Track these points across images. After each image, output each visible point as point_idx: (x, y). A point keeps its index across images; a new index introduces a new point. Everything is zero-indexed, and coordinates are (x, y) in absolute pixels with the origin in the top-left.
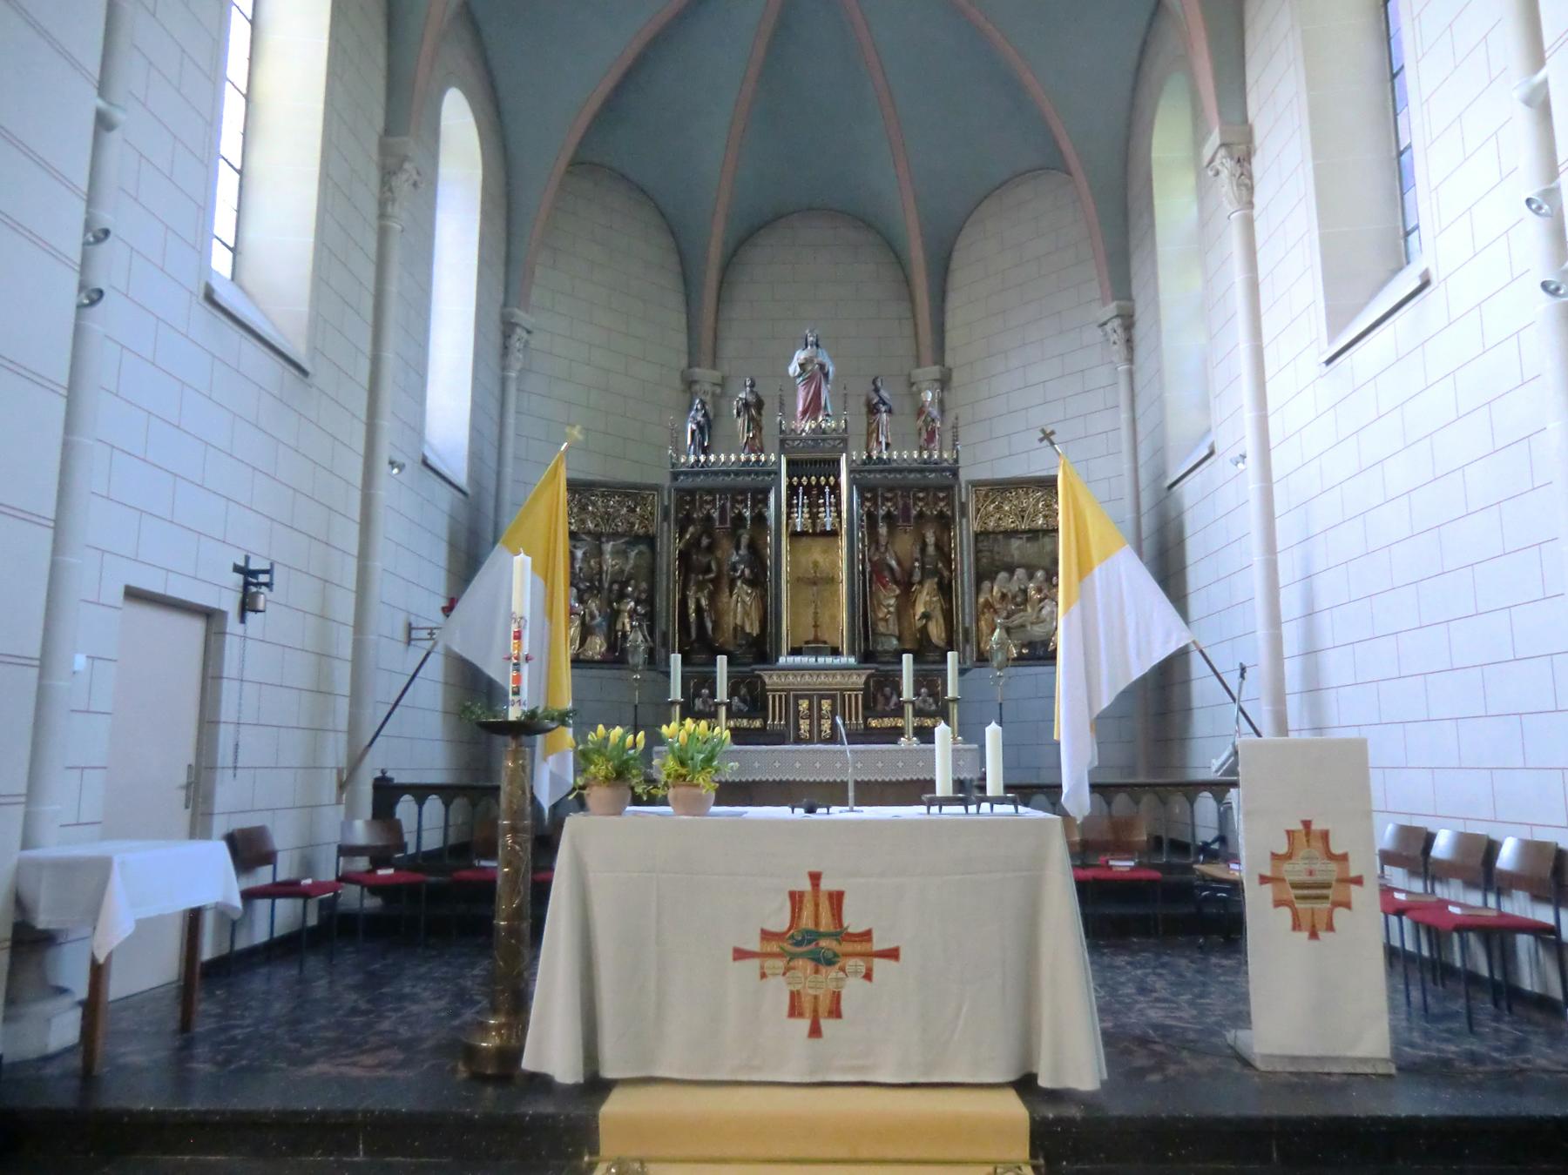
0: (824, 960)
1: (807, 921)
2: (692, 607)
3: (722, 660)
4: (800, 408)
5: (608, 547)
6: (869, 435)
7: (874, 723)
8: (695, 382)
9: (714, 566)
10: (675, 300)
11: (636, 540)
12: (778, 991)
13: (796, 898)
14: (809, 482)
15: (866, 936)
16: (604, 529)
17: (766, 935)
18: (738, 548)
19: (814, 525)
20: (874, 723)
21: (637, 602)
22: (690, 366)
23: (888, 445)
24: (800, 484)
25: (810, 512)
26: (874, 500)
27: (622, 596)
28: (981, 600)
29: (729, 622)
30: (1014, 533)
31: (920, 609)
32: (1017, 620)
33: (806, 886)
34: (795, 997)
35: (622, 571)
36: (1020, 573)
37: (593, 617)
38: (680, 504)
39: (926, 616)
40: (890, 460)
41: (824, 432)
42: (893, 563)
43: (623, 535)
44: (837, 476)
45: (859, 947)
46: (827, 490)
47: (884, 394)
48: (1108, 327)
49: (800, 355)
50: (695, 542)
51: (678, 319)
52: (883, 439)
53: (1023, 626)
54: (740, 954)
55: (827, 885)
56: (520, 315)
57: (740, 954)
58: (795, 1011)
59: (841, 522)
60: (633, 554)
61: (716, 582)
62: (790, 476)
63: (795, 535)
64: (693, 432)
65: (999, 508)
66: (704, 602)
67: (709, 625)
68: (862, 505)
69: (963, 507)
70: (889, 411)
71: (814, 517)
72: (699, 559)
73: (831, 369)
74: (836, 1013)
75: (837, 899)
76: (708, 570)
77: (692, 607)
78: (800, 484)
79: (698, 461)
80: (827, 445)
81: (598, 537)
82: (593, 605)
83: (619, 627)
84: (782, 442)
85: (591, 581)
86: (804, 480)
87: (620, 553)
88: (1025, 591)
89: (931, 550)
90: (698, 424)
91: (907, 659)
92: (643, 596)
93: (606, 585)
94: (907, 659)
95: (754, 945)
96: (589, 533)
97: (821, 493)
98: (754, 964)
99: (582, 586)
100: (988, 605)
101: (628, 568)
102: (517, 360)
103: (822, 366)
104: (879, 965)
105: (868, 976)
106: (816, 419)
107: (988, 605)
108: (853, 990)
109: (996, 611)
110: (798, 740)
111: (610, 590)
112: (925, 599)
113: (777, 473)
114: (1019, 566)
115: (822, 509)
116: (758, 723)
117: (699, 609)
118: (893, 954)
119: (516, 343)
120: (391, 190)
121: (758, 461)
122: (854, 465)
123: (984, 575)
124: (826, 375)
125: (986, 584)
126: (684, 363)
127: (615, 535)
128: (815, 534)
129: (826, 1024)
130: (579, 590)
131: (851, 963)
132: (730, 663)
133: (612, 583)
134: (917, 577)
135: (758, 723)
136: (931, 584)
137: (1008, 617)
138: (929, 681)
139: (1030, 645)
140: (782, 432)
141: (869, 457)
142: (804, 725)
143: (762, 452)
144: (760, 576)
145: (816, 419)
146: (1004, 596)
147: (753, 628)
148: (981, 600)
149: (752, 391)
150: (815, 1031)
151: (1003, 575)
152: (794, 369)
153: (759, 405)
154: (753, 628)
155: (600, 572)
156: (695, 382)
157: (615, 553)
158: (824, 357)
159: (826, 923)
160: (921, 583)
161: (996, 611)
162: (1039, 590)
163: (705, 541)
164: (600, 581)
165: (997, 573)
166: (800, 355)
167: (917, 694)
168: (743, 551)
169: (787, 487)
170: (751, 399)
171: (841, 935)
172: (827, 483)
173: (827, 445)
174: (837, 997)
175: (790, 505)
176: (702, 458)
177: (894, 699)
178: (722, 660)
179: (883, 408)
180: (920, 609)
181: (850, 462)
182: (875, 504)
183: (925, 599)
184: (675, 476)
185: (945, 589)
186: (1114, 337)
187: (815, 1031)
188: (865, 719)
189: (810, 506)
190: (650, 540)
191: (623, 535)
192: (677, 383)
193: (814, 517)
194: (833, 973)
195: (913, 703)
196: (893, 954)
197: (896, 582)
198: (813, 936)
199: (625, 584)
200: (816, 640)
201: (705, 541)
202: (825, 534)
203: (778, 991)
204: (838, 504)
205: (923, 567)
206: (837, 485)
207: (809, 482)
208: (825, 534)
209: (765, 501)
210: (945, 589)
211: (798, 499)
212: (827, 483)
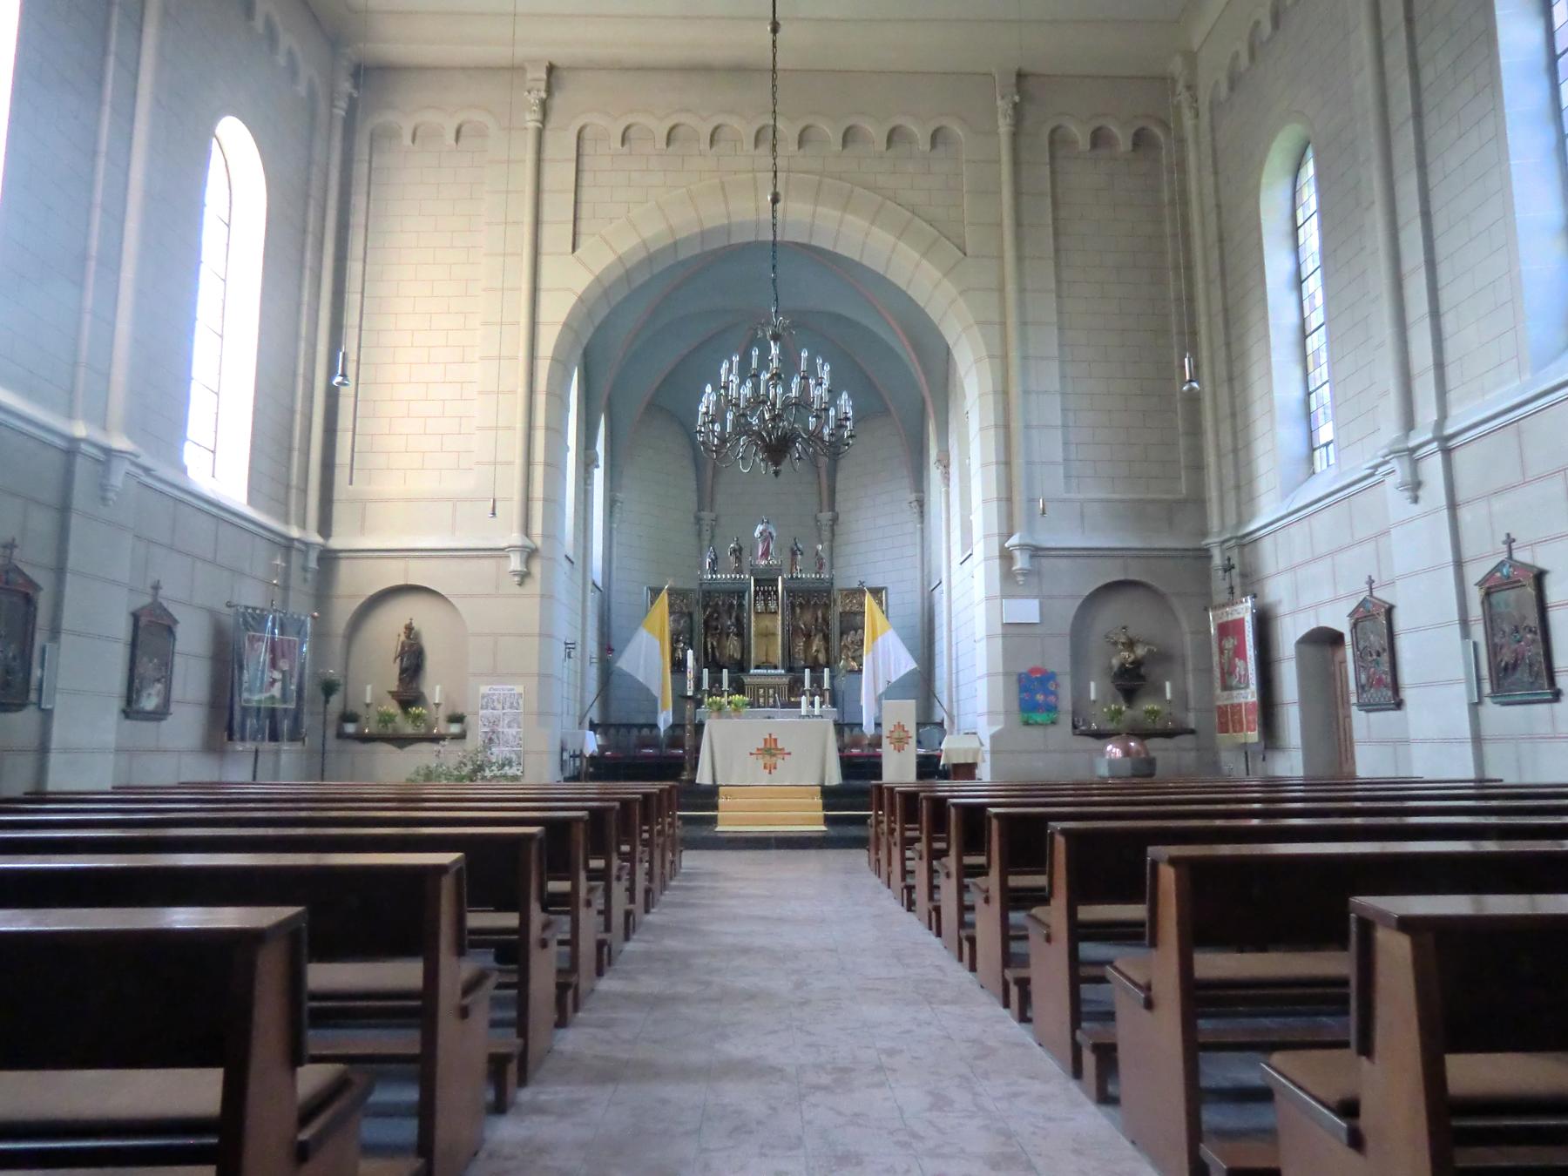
0: (774, 755)
1: (768, 746)
2: (709, 646)
3: (725, 671)
4: (760, 553)
6: (792, 565)
7: (793, 699)
8: (702, 519)
9: (719, 627)
12: (761, 763)
13: (765, 740)
17: (758, 749)
18: (730, 618)
19: (766, 609)
20: (793, 699)
22: (699, 510)
23: (800, 570)
24: (760, 590)
26: (794, 597)
28: (842, 644)
31: (814, 648)
33: (768, 737)
34: (765, 764)
35: (677, 630)
38: (704, 596)
39: (817, 651)
40: (801, 578)
41: (771, 566)
42: (803, 626)
47: (800, 546)
48: (912, 505)
49: (760, 528)
50: (711, 615)
51: (693, 484)
52: (798, 568)
54: (751, 754)
55: (773, 737)
56: (620, 496)
57: (751, 754)
58: (765, 768)
60: (682, 622)
61: (720, 634)
62: (755, 586)
63: (757, 613)
64: (709, 563)
66: (715, 643)
67: (717, 654)
68: (788, 599)
69: (835, 600)
70: (802, 554)
71: (766, 605)
73: (774, 534)
74: (775, 768)
75: (775, 740)
76: (716, 628)
77: (709, 646)
79: (712, 577)
83: (677, 655)
84: (752, 570)
86: (762, 589)
89: (820, 620)
90: (712, 559)
91: (807, 671)
94: (807, 671)
97: (769, 592)
100: (845, 646)
101: (679, 628)
102: (617, 516)
103: (770, 533)
104: (786, 757)
106: (767, 559)
107: (845, 646)
108: (780, 762)
109: (849, 649)
110: (759, 707)
112: (817, 644)
118: (789, 754)
119: (616, 510)
121: (740, 578)
124: (772, 538)
125: (845, 637)
131: (779, 756)
132: (729, 672)
134: (813, 634)
136: (820, 636)
137: (854, 652)
138: (817, 681)
140: (751, 565)
141: (792, 576)
142: (761, 700)
143: (742, 573)
144: (742, 632)
145: (767, 559)
146: (853, 642)
147: (737, 656)
148: (842, 644)
149: (737, 544)
150: (770, 773)
151: (852, 632)
152: (757, 534)
153: (741, 549)
154: (737, 656)
156: (702, 519)
158: (772, 529)
159: (773, 746)
160: (815, 635)
161: (849, 649)
163: (715, 615)
166: (760, 528)
167: (811, 686)
168: (733, 620)
170: (737, 547)
171: (777, 749)
172: (772, 590)
174: (775, 764)
175: (755, 600)
176: (714, 576)
177: (801, 689)
178: (725, 671)
179: (798, 553)
180: (814, 648)
181: (783, 580)
182: (794, 598)
183: (817, 644)
185: (826, 638)
186: (915, 510)
187: (770, 773)
188: (789, 697)
189: (764, 600)
190: (690, 615)
193: (766, 605)
194: (775, 759)
195: (810, 690)
196: (789, 754)
197: (804, 635)
198: (770, 749)
199: (679, 635)
200: (767, 661)
201: (715, 615)
202: (771, 613)
203: (761, 763)
204: (777, 599)
205: (816, 628)
206: (777, 591)
208: (771, 613)
209: (744, 596)
210: (826, 638)
212: (772, 590)
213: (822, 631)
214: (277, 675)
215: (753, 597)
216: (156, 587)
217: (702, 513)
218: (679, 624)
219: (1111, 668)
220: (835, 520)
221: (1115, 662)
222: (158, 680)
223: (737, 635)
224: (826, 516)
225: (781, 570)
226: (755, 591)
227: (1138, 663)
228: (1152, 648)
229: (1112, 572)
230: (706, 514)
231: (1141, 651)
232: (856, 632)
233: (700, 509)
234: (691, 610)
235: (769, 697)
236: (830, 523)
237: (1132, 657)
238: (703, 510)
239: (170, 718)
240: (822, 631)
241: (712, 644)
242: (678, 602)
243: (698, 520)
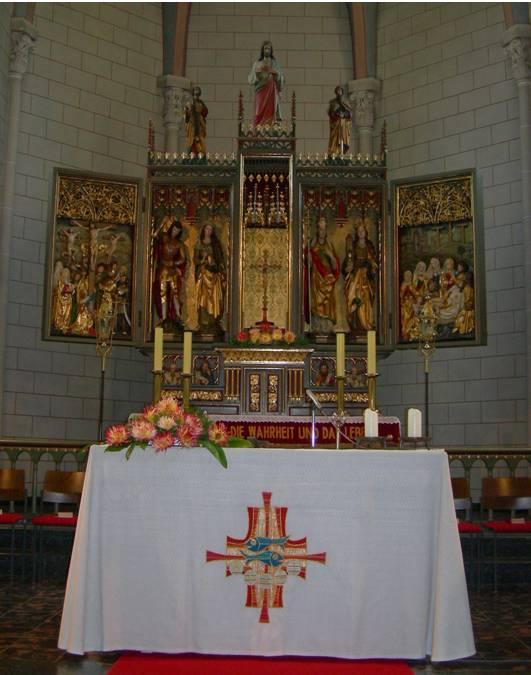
0: (272, 562)
5: (95, 233)
8: (170, 88)
9: (182, 254)
13: (252, 513)
14: (263, 180)
15: (302, 542)
17: (231, 542)
22: (165, 73)
24: (255, 180)
25: (263, 206)
26: (316, 197)
27: (106, 279)
28: (403, 288)
34: (250, 589)
36: (434, 262)
38: (155, 194)
42: (331, 255)
43: (110, 222)
44: (286, 174)
45: (301, 552)
46: (278, 187)
54: (211, 556)
57: (211, 556)
58: (250, 602)
59: (288, 216)
60: (115, 241)
62: (247, 174)
68: (306, 201)
69: (390, 206)
74: (279, 603)
75: (282, 512)
78: (255, 180)
80: (277, 146)
85: (81, 263)
88: (436, 279)
89: (362, 242)
92: (124, 279)
93: (93, 267)
95: (221, 548)
97: (272, 189)
98: (221, 565)
99: (73, 267)
104: (312, 567)
105: (302, 575)
107: (408, 292)
108: (291, 583)
111: (97, 273)
113: (236, 170)
114: (434, 256)
115: (273, 204)
122: (300, 165)
123: (406, 265)
126: (159, 70)
128: (267, 226)
129: (272, 612)
130: (71, 271)
133: (98, 266)
134: (350, 267)
136: (362, 272)
148: (403, 288)
156: (170, 88)
159: (274, 534)
160: (353, 272)
162: (448, 277)
163: (175, 231)
164: (89, 263)
165: (416, 262)
169: (245, 183)
172: (278, 180)
173: (277, 146)
174: (280, 589)
175: (246, 200)
182: (317, 200)
184: (152, 172)
189: (262, 200)
190: (131, 229)
191: (110, 222)
192: (153, 89)
193: (266, 211)
194: (279, 572)
198: (263, 545)
199: (107, 267)
201: (175, 231)
204: (286, 200)
205: (355, 258)
206: (286, 182)
207: (263, 180)
208: (274, 226)
209: (226, 196)
211: (253, 195)
212: (278, 180)
213: (366, 264)
215: (241, 195)
217: (169, 76)
218: (110, 245)
223: (214, 270)
225: (293, 143)
226: (247, 182)
232: (428, 263)
234: (133, 219)
238: (171, 73)
240: (366, 264)
241: (168, 284)
242: (111, 201)
243: (163, 87)
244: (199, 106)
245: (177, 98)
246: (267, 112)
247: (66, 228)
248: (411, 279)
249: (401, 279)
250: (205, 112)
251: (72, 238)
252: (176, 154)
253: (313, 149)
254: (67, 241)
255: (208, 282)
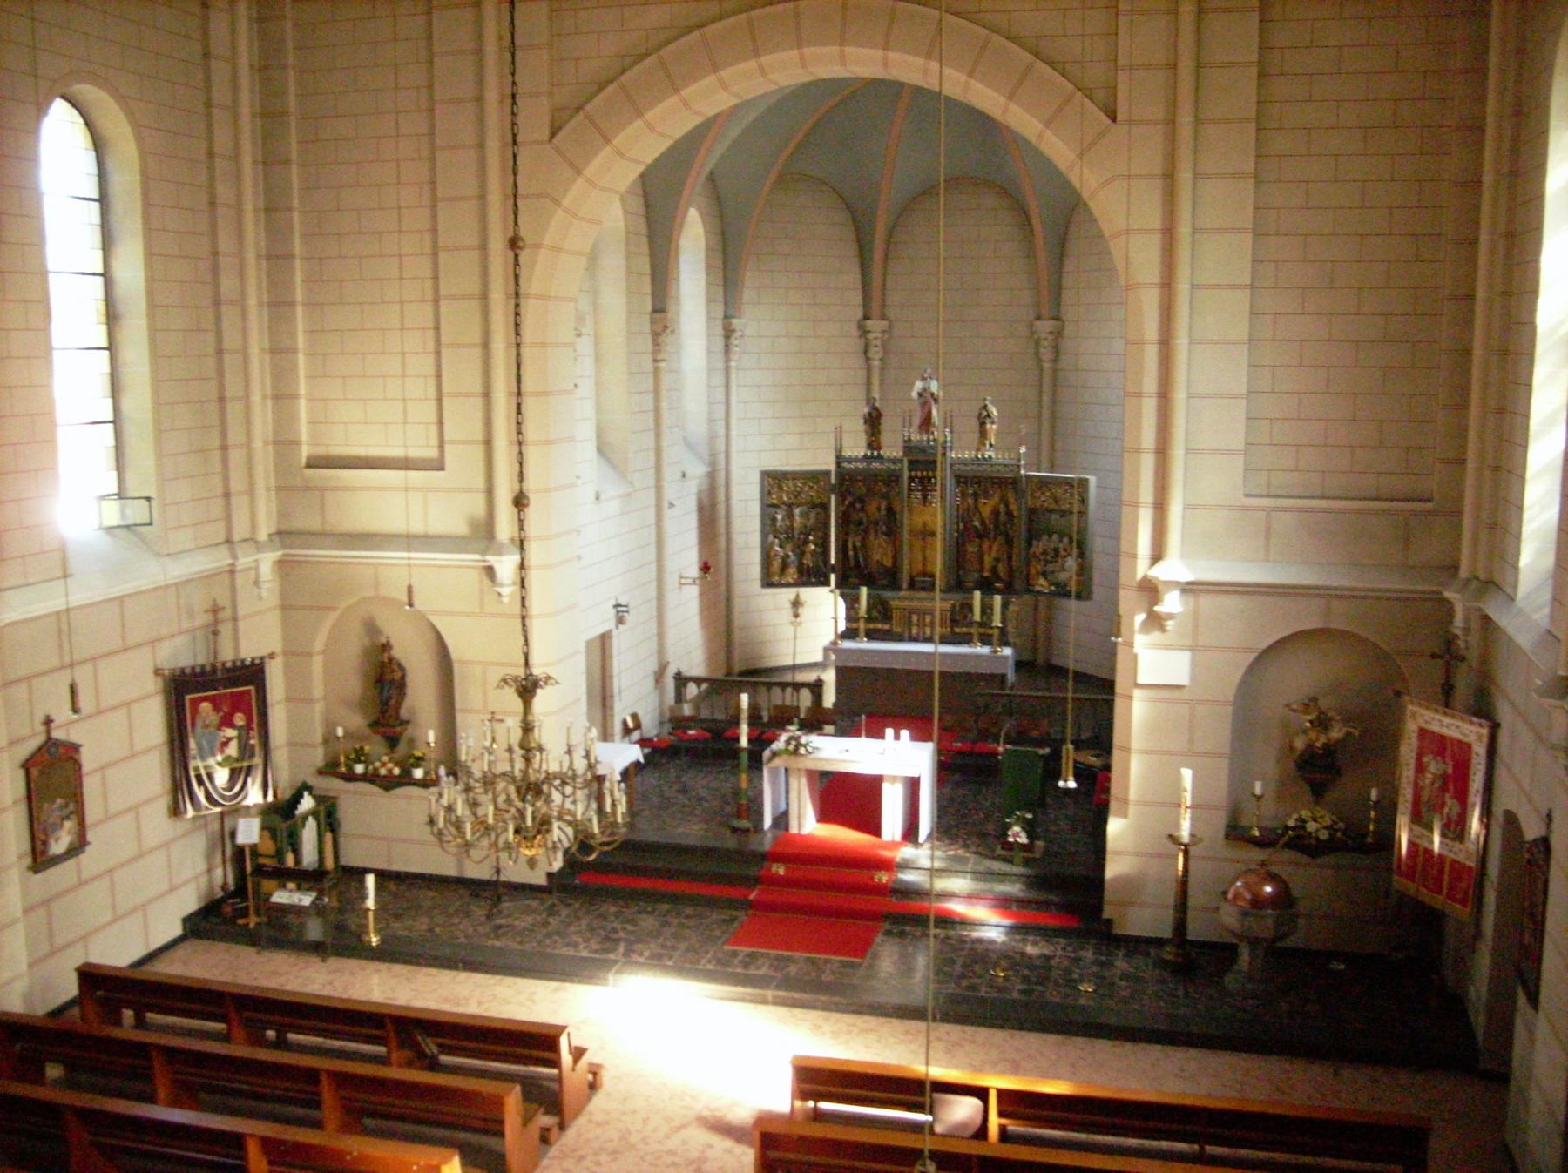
5: (797, 511)
7: (957, 630)
10: (851, 250)
11: (814, 506)
16: (793, 501)
20: (957, 630)
21: (816, 545)
27: (806, 542)
29: (876, 557)
30: (1051, 511)
32: (1050, 567)
36: (1055, 537)
37: (788, 556)
50: (852, 505)
51: (854, 277)
53: (1053, 572)
61: (866, 531)
62: (910, 471)
65: (1043, 493)
66: (858, 544)
67: (861, 559)
72: (855, 516)
81: (790, 506)
82: (789, 547)
87: (804, 515)
96: (784, 503)
116: (887, 627)
117: (855, 547)
119: (734, 341)
120: (658, 345)
123: (1032, 536)
126: (860, 314)
127: (798, 505)
134: (992, 534)
135: (887, 627)
136: (1001, 539)
139: (1057, 585)
142: (914, 631)
144: (892, 532)
147: (888, 563)
151: (1045, 537)
154: (888, 563)
155: (792, 528)
157: (802, 515)
158: (934, 386)
160: (995, 538)
166: (919, 385)
175: (910, 489)
184: (838, 464)
185: (1009, 542)
188: (952, 628)
190: (825, 507)
192: (854, 332)
210: (1009, 542)
214: (231, 733)
216: (48, 722)
219: (1292, 748)
220: (1058, 334)
221: (1300, 743)
222: (68, 818)
223: (887, 534)
224: (1045, 327)
227: (1329, 749)
228: (1352, 730)
229: (1310, 620)
230: (875, 325)
231: (1336, 733)
232: (1050, 536)
233: (866, 318)
235: (925, 625)
236: (1050, 337)
237: (1323, 740)
239: (88, 849)
242: (806, 489)
243: (864, 332)
244: (874, 414)
245: (876, 338)
246: (926, 423)
247: (774, 510)
248: (1039, 547)
249: (1030, 545)
250: (879, 415)
251: (779, 517)
252: (856, 447)
253: (961, 453)
254: (774, 520)
255: (884, 544)
